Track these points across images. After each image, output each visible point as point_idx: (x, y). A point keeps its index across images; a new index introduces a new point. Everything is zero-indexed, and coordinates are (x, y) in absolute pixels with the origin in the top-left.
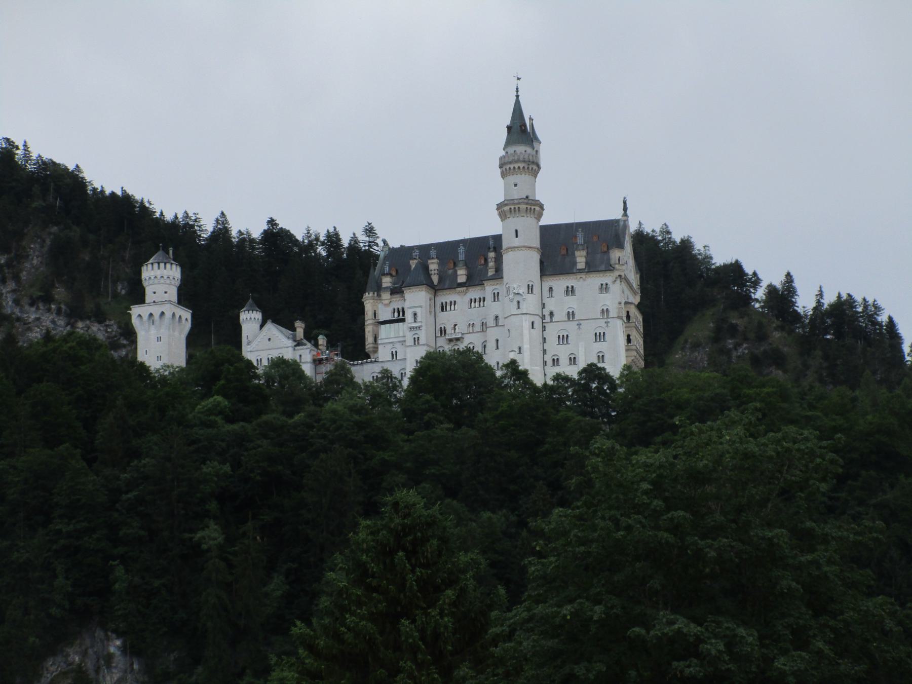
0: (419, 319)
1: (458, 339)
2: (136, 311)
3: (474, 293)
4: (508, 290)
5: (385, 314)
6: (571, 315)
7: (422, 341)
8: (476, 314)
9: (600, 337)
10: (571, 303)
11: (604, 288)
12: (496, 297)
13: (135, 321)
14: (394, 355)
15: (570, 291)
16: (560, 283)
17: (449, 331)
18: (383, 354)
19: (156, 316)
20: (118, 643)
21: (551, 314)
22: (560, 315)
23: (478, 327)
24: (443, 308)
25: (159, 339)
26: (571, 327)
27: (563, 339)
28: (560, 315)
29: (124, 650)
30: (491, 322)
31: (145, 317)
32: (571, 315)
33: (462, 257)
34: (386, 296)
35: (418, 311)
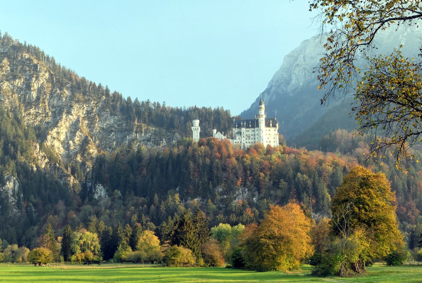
2: (192, 128)
3: (252, 129)
5: (236, 131)
6: (270, 134)
8: (253, 133)
11: (275, 130)
12: (257, 130)
13: (193, 130)
14: (239, 139)
15: (269, 130)
16: (268, 129)
17: (248, 135)
19: (197, 129)
22: (268, 134)
23: (253, 135)
24: (247, 131)
28: (268, 134)
30: (256, 134)
31: (195, 129)
33: (250, 123)
34: (237, 128)
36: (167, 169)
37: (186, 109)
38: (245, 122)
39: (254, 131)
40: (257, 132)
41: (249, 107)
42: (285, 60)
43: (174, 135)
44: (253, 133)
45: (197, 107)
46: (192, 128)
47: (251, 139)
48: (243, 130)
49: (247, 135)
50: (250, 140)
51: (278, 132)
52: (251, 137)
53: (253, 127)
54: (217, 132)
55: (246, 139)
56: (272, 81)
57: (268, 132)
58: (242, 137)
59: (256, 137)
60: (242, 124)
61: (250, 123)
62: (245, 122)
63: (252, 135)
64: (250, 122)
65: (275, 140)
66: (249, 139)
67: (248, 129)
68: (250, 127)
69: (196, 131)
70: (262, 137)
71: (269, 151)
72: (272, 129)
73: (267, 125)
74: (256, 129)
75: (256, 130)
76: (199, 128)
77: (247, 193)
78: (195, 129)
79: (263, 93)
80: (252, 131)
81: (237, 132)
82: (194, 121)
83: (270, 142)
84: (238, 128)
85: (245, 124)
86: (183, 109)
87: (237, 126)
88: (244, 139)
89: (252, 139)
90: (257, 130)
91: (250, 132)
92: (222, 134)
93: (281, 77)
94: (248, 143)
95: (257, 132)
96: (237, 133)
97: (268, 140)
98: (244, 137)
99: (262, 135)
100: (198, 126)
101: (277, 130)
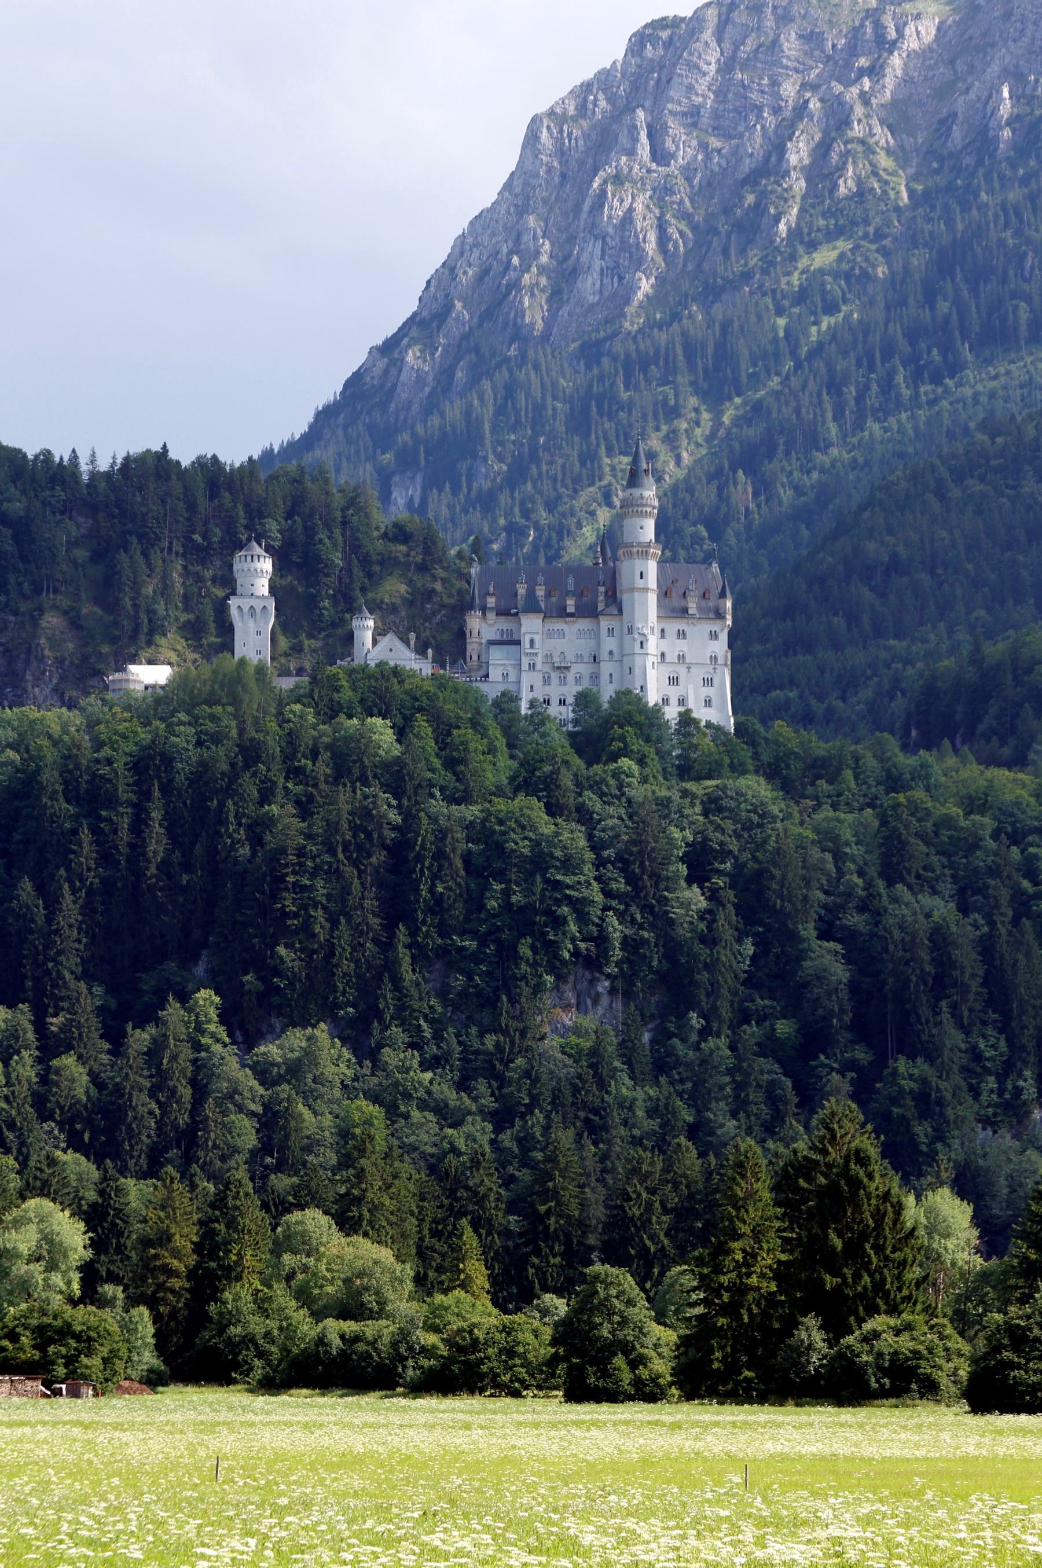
0: (537, 644)
1: (567, 668)
4: (630, 630)
6: (681, 658)
7: (539, 667)
9: (708, 682)
10: (682, 646)
11: (714, 636)
12: (611, 632)
13: (234, 612)
15: (681, 634)
16: (673, 626)
18: (495, 674)
20: (607, 984)
21: (663, 655)
24: (550, 634)
25: (259, 633)
26: (682, 671)
27: (674, 681)
29: (612, 991)
30: (604, 655)
31: (246, 610)
32: (681, 658)
34: (491, 616)
35: (537, 638)
36: (137, 848)
37: (103, 466)
38: (541, 579)
39: (597, 634)
40: (609, 644)
41: (299, 426)
42: (532, 138)
43: (35, 623)
44: (585, 646)
45: (173, 455)
46: (233, 602)
47: (570, 676)
48: (531, 625)
49: (549, 657)
50: (565, 690)
51: (730, 646)
52: (576, 669)
53: (588, 611)
54: (379, 633)
55: (547, 681)
56: (449, 267)
57: (675, 647)
58: (525, 666)
59: (607, 668)
60: (522, 590)
61: (571, 587)
62: (541, 579)
63: (579, 658)
64: (571, 580)
65: (710, 691)
66: (563, 682)
67: (558, 625)
68: (570, 609)
69: (251, 624)
70: (637, 672)
71: (690, 756)
72: (699, 630)
73: (674, 606)
74: (605, 623)
75: (604, 632)
76: (272, 604)
77: (605, 1000)
78: (246, 610)
79: (390, 348)
80: (580, 633)
81: (493, 637)
82: (239, 565)
83: (682, 702)
84: (503, 612)
85: (540, 592)
86: (84, 467)
87: (491, 601)
88: (537, 678)
89: (578, 680)
90: (611, 632)
91: (569, 639)
92: (406, 642)
93: (505, 250)
94: (554, 701)
95: (609, 644)
96: (491, 643)
97: (674, 693)
98: (532, 667)
99: (638, 660)
100: (265, 591)
101: (724, 637)
